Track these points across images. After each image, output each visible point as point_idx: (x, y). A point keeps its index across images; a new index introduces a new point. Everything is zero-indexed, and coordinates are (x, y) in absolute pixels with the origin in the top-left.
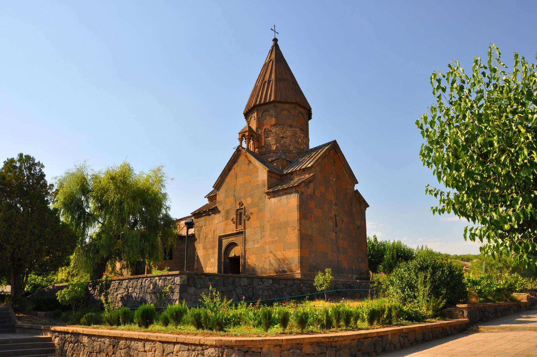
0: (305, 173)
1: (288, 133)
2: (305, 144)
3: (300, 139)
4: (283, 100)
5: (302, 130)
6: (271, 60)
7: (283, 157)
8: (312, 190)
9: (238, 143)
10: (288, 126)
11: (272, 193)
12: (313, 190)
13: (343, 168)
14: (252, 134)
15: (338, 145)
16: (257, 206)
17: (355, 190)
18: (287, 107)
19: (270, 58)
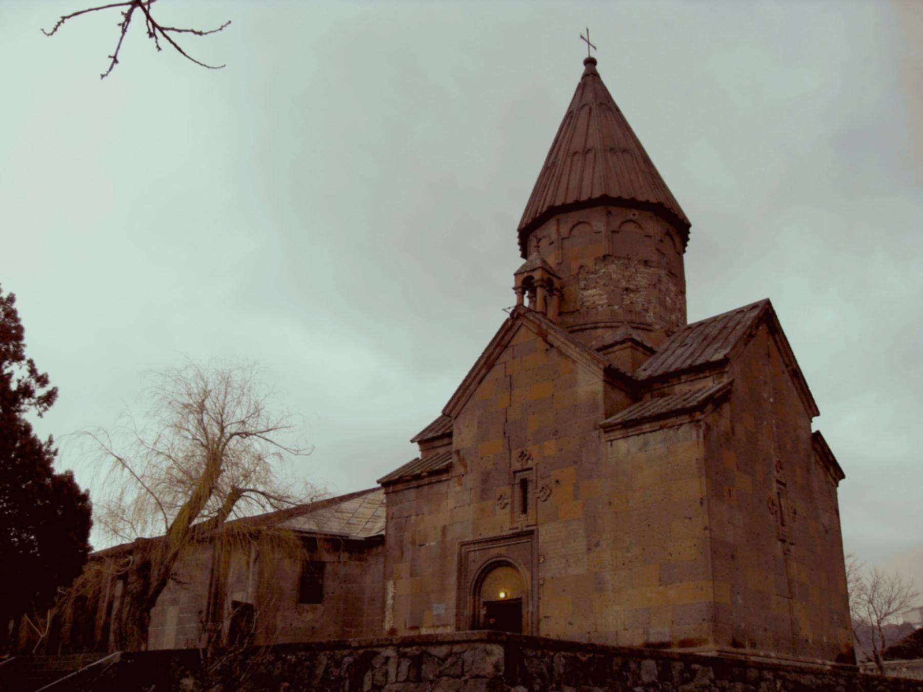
0: (705, 377)
3: (669, 295)
4: (626, 196)
10: (639, 261)
11: (619, 426)
12: (731, 421)
14: (551, 276)
16: (575, 463)
17: (814, 431)
19: (580, 101)
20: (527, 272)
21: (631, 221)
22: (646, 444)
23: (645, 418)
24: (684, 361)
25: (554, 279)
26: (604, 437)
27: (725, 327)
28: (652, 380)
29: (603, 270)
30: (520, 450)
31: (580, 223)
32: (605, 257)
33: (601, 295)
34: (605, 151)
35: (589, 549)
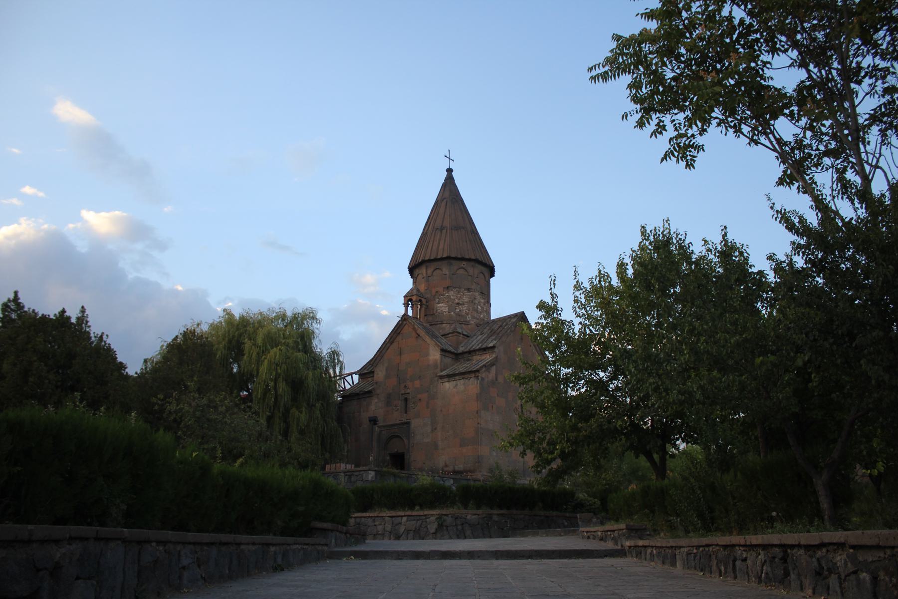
0: (486, 353)
1: (465, 299)
2: (486, 311)
3: (480, 306)
4: (459, 256)
5: (483, 293)
6: (445, 198)
7: (460, 330)
8: (494, 375)
9: (403, 312)
12: (496, 375)
13: (532, 346)
14: (421, 298)
15: (526, 317)
16: (428, 392)
18: (464, 265)
20: (410, 296)
21: (462, 268)
22: (457, 385)
23: (457, 374)
24: (478, 345)
25: (423, 299)
26: (440, 381)
27: (501, 326)
28: (463, 353)
29: (447, 294)
30: (404, 384)
31: (437, 269)
32: (448, 287)
33: (444, 307)
34: (452, 229)
35: (432, 431)
